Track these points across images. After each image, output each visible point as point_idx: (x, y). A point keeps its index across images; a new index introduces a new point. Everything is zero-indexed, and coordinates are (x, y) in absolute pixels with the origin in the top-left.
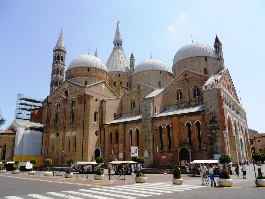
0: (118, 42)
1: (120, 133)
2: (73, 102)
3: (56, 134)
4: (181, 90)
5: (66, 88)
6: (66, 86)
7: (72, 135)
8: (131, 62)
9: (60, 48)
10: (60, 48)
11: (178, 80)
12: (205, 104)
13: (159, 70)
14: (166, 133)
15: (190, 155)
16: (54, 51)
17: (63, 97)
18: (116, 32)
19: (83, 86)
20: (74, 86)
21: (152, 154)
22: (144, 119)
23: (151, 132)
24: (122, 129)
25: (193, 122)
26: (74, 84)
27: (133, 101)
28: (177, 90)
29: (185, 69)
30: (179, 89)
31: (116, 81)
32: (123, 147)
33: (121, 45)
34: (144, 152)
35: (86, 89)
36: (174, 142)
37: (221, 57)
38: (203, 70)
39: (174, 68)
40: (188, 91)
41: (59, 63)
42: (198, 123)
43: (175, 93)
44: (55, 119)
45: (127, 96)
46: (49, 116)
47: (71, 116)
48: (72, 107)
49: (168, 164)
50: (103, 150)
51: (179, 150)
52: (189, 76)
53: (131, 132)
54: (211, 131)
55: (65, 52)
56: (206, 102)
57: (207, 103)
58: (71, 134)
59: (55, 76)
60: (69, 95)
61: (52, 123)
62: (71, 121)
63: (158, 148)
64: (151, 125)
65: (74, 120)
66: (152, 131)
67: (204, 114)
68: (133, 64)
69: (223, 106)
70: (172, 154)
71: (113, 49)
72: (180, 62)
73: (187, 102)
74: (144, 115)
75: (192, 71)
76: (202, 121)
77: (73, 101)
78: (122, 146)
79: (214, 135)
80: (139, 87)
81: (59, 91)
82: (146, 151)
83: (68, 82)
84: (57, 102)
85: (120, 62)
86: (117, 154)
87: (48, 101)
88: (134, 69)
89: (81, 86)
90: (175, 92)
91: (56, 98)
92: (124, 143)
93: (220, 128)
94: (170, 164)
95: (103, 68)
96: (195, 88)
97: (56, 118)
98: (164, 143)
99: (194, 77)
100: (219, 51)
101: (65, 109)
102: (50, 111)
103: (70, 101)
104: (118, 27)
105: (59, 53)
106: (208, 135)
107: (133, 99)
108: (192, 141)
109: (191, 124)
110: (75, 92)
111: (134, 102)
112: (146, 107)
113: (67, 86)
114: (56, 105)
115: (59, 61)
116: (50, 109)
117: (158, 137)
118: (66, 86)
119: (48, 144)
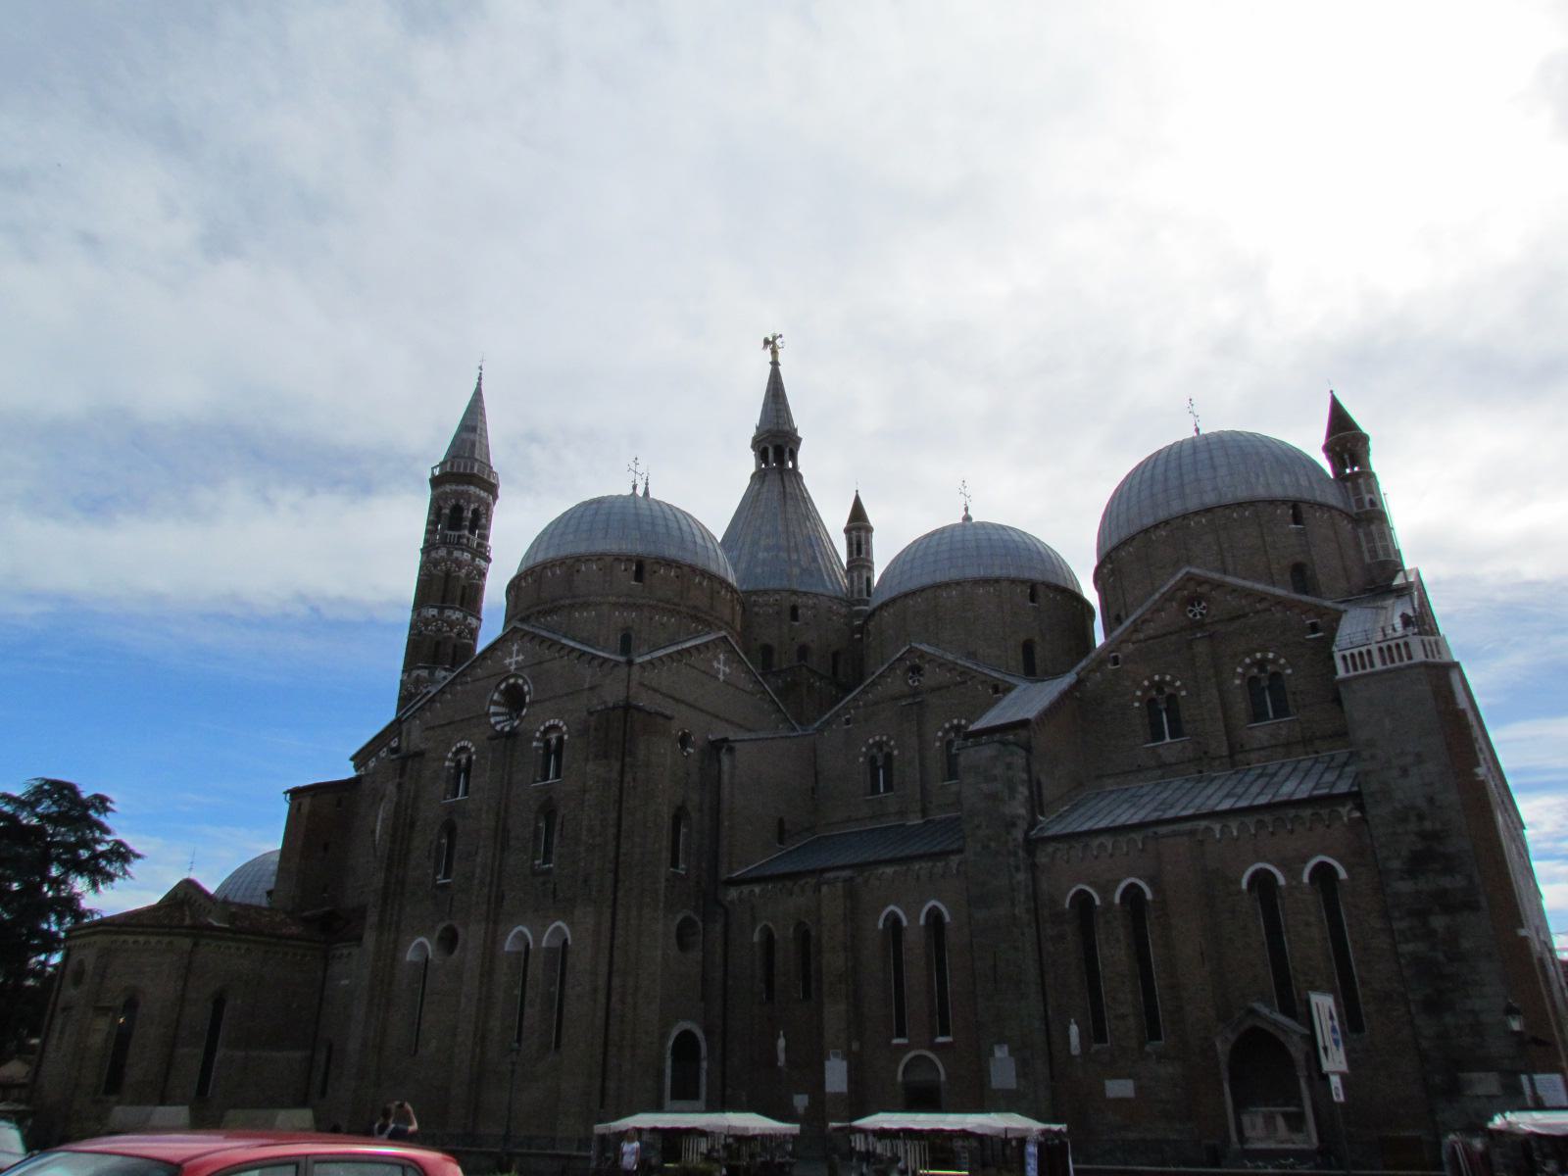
0: (779, 442)
3: (441, 938)
4: (1171, 684)
5: (513, 667)
7: (544, 944)
8: (850, 545)
9: (465, 468)
10: (465, 468)
11: (1150, 629)
13: (1023, 582)
16: (436, 482)
17: (493, 720)
19: (612, 657)
20: (562, 657)
25: (1293, 873)
26: (564, 646)
27: (886, 749)
28: (1149, 688)
29: (1184, 571)
30: (1157, 678)
33: (793, 456)
34: (992, 1054)
37: (1372, 503)
38: (1287, 576)
40: (1215, 692)
41: (458, 544)
42: (1323, 873)
43: (1137, 704)
45: (848, 722)
46: (403, 826)
47: (537, 829)
48: (546, 778)
51: (1222, 1048)
59: (434, 612)
62: (537, 862)
65: (556, 850)
67: (1364, 820)
68: (864, 551)
71: (753, 476)
72: (1146, 531)
74: (978, 827)
75: (1229, 579)
77: (554, 742)
80: (916, 670)
81: (469, 687)
82: (1006, 1048)
83: (526, 639)
84: (454, 749)
85: (792, 544)
87: (404, 745)
88: (869, 581)
89: (606, 660)
90: (1140, 699)
91: (449, 724)
95: (713, 568)
99: (1247, 610)
100: (1354, 476)
103: (535, 744)
104: (775, 364)
105: (462, 494)
106: (1407, 948)
107: (885, 738)
110: (567, 695)
111: (889, 757)
112: (995, 778)
113: (521, 658)
114: (447, 764)
115: (461, 533)
118: (514, 659)
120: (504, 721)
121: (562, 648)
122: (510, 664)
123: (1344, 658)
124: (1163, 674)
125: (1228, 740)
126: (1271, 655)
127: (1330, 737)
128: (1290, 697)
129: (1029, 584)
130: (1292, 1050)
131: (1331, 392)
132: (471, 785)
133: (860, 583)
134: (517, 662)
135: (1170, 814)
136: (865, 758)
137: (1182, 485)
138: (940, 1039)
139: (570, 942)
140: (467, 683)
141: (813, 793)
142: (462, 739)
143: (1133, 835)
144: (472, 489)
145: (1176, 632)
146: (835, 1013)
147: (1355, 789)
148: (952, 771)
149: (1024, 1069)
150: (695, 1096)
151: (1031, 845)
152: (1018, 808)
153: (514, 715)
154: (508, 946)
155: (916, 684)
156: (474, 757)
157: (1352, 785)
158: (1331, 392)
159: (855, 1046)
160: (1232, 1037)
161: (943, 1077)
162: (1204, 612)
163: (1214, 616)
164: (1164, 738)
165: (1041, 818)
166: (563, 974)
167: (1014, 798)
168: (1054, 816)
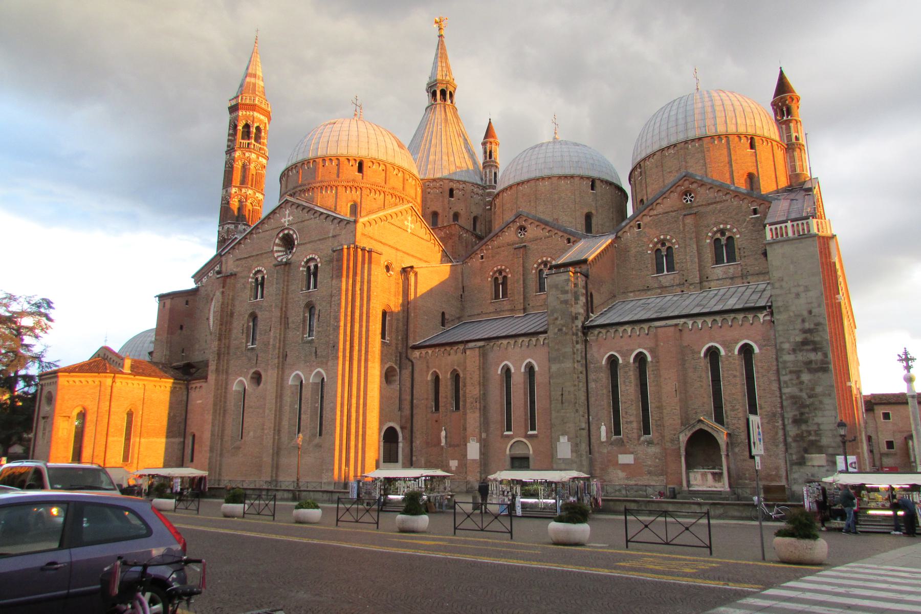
0: (444, 87)
1: (471, 378)
2: (312, 273)
3: (252, 378)
5: (286, 224)
6: (287, 219)
7: (311, 381)
8: (485, 152)
12: (777, 285)
13: (588, 178)
14: (632, 377)
15: (723, 453)
17: (276, 255)
18: (437, 54)
21: (584, 447)
22: (556, 330)
23: (580, 375)
24: (477, 363)
25: (728, 346)
26: (316, 212)
27: (504, 274)
28: (657, 243)
30: (662, 237)
31: (440, 211)
32: (480, 425)
33: (451, 95)
34: (559, 441)
35: (359, 226)
36: (665, 411)
37: (797, 139)
39: (638, 171)
40: (695, 246)
43: (649, 252)
44: (248, 327)
45: (482, 258)
46: (226, 316)
48: (309, 288)
49: (640, 483)
50: (407, 432)
51: (683, 438)
52: (698, 197)
53: (507, 371)
54: (798, 377)
55: (267, 114)
56: (781, 279)
57: (784, 284)
58: (307, 379)
60: (299, 248)
61: (235, 340)
62: (305, 336)
63: (603, 428)
64: (581, 353)
66: (584, 372)
68: (493, 157)
69: (837, 296)
70: (652, 450)
72: (663, 150)
73: (690, 281)
74: (556, 319)
76: (764, 343)
77: (312, 268)
78: (478, 419)
79: (808, 391)
80: (522, 228)
81: (260, 235)
82: (566, 437)
83: (294, 207)
86: (458, 446)
87: (224, 269)
92: (484, 411)
93: (831, 366)
94: (646, 483)
96: (718, 235)
97: (251, 324)
98: (626, 413)
101: (284, 296)
102: (230, 302)
103: (301, 269)
105: (247, 117)
107: (503, 267)
108: (726, 407)
109: (723, 352)
110: (320, 240)
111: (505, 278)
112: (566, 292)
116: (231, 294)
117: (605, 391)
118: (287, 219)
119: (225, 411)
120: (282, 256)
121: (315, 213)
122: (285, 222)
123: (771, 230)
124: (665, 235)
125: (700, 274)
126: (728, 227)
127: (757, 274)
128: (737, 250)
129: (591, 180)
130: (720, 441)
131: (781, 68)
132: (265, 292)
133: (490, 175)
134: (289, 221)
135: (664, 315)
136: (492, 279)
137: (686, 123)
138: (530, 433)
139: (325, 380)
140: (259, 233)
141: (461, 298)
142: (258, 266)
143: (643, 326)
144: (256, 114)
145: (675, 211)
146: (473, 419)
147: (769, 304)
148: (541, 288)
149: (575, 448)
150: (397, 461)
151: (586, 330)
152: (580, 309)
153: (288, 252)
154: (290, 382)
155: (523, 236)
156: (266, 277)
157: (767, 302)
158: (781, 68)
159: (484, 435)
160: (689, 434)
161: (531, 452)
162: (693, 199)
163: (698, 202)
164: (663, 272)
165: (591, 314)
166: (322, 397)
167: (577, 303)
168: (599, 313)
